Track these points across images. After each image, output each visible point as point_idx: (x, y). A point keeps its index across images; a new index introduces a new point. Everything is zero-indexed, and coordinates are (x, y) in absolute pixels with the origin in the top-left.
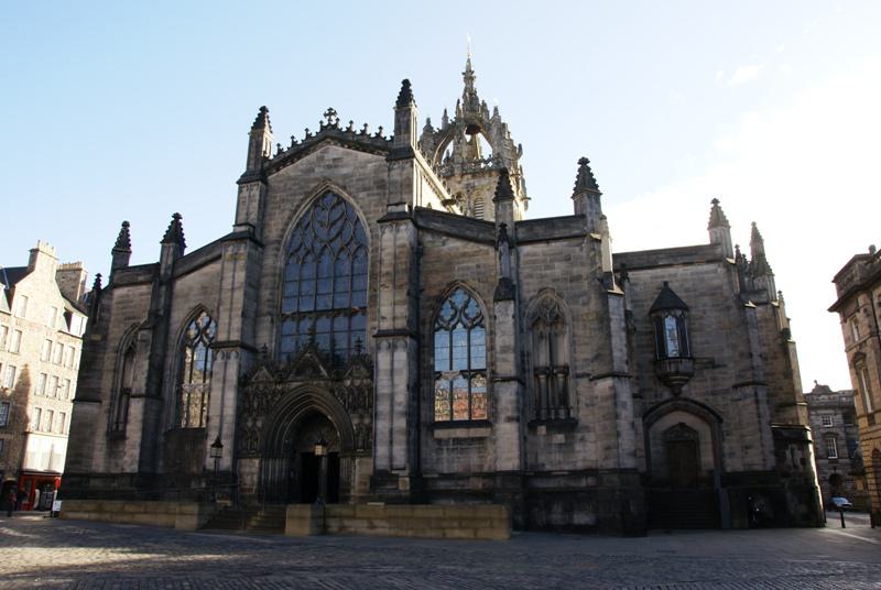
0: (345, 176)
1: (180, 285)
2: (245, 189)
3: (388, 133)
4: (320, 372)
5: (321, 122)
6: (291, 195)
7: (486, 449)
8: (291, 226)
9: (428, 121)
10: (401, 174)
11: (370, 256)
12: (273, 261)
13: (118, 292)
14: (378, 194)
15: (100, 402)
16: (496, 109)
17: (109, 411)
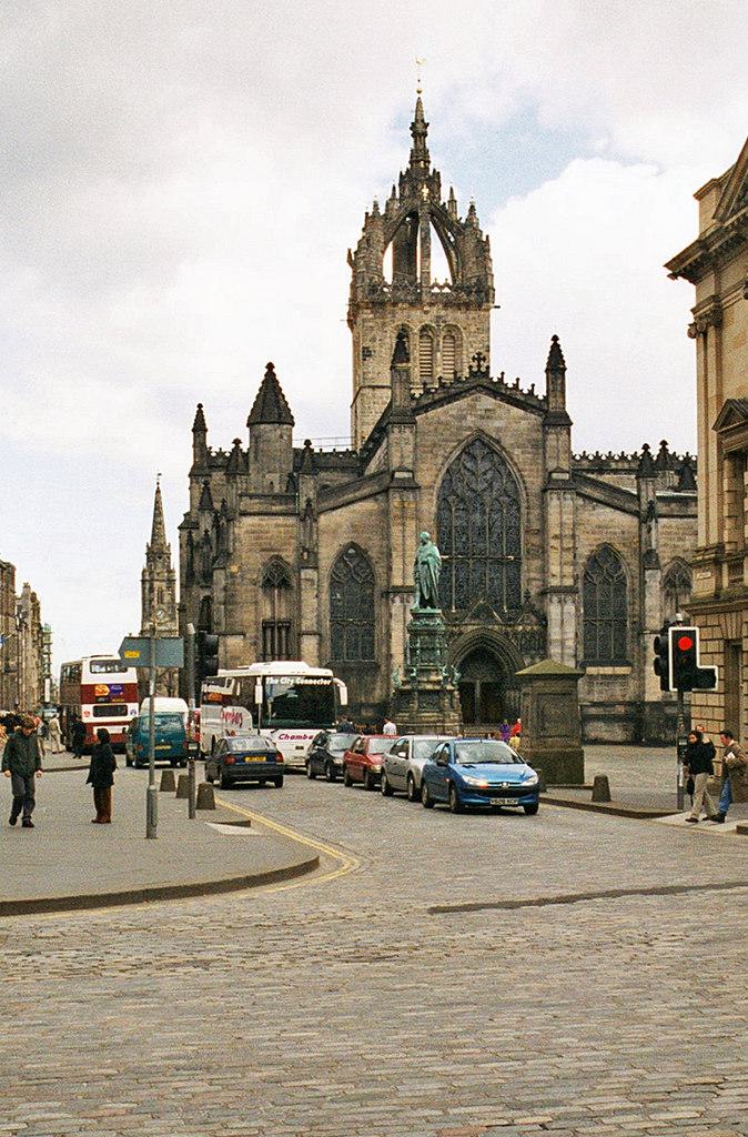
0: (498, 430)
1: (323, 519)
2: (396, 430)
3: (541, 392)
4: (493, 617)
5: (470, 367)
6: (444, 440)
7: (627, 684)
8: (444, 471)
9: (376, 206)
10: (558, 440)
11: (523, 510)
12: (429, 506)
13: (248, 521)
14: (532, 453)
15: (244, 635)
16: (472, 208)
17: (255, 644)
